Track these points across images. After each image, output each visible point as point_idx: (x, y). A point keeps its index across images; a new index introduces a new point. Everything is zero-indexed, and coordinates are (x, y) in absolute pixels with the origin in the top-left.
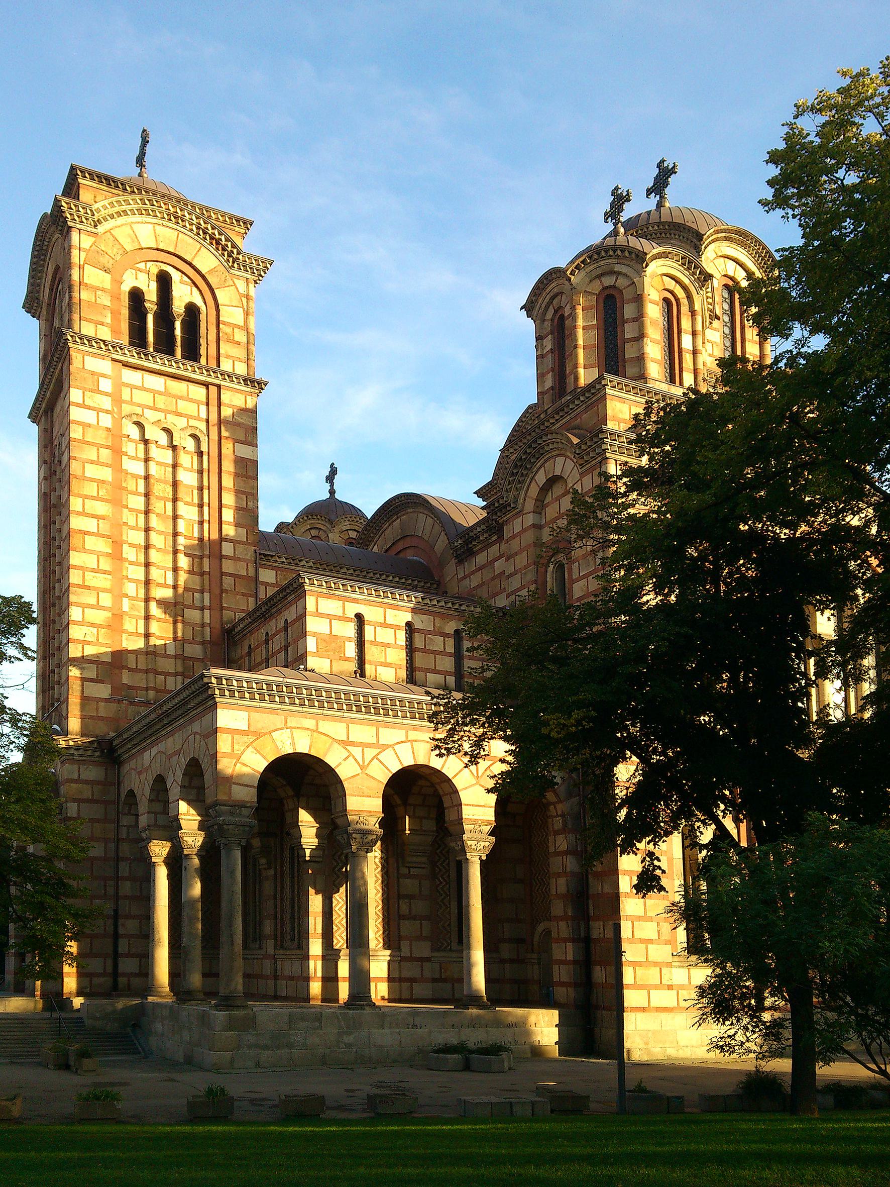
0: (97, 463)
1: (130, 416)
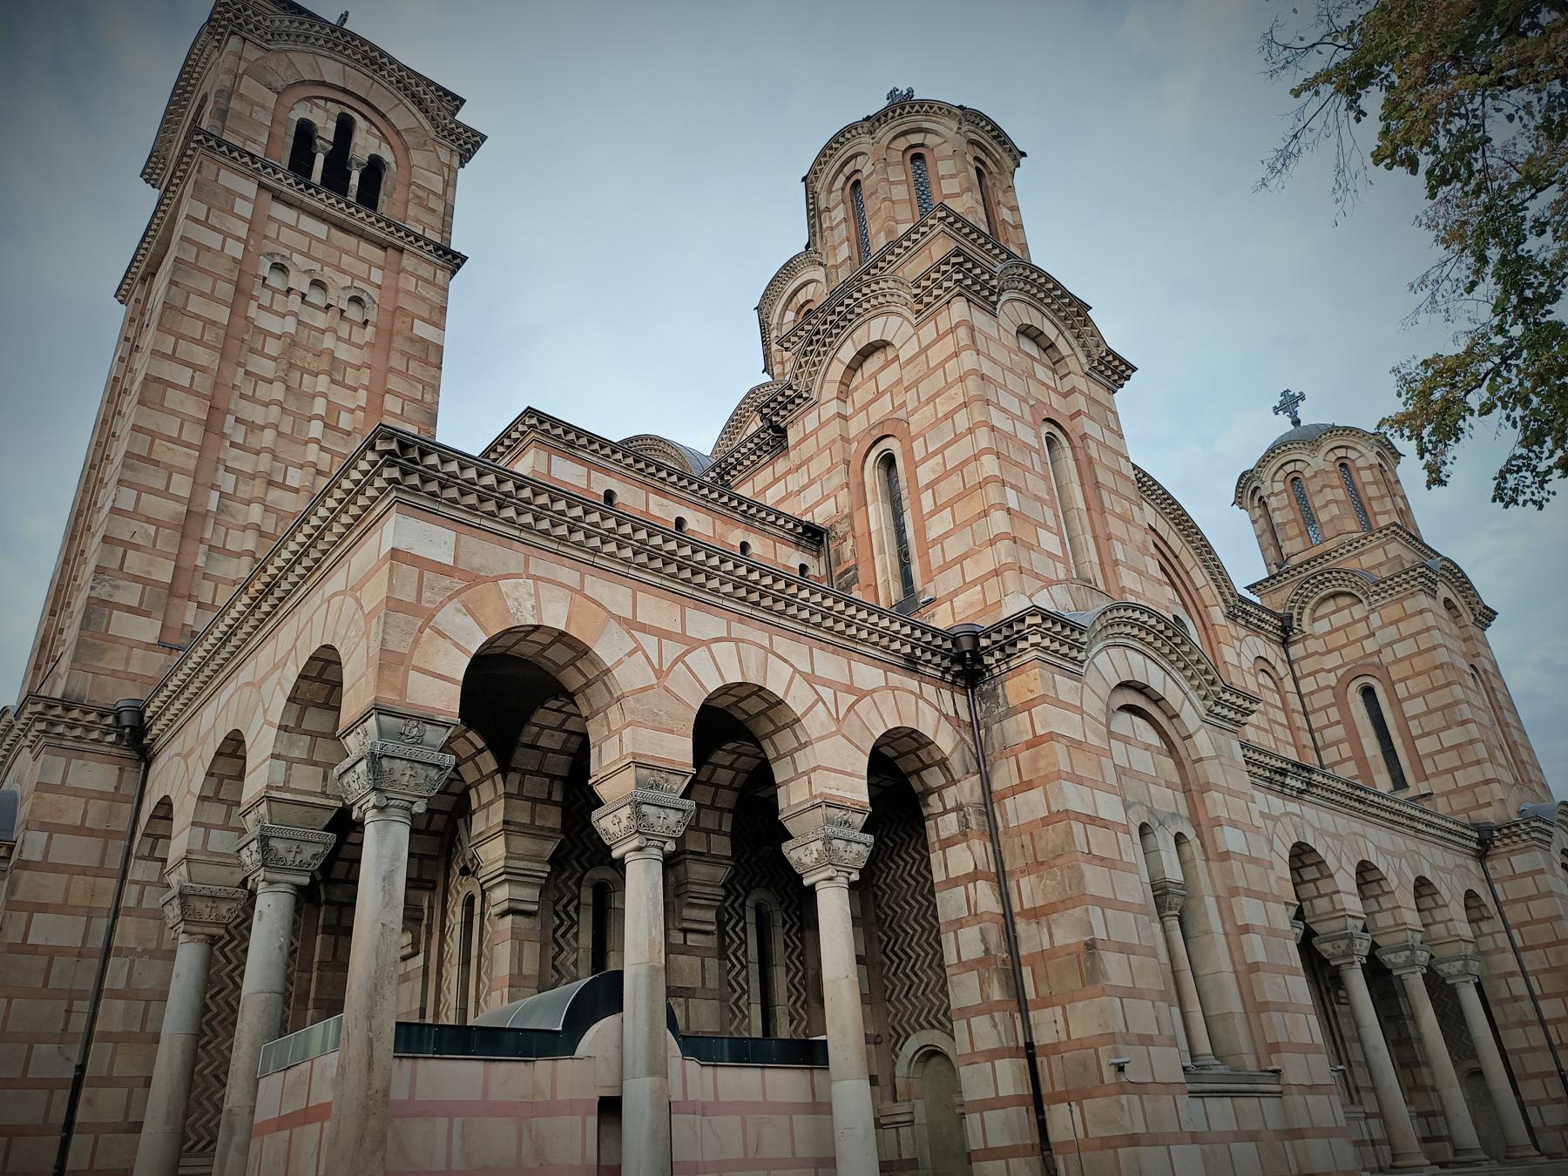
0: (210, 297)
1: (272, 254)
